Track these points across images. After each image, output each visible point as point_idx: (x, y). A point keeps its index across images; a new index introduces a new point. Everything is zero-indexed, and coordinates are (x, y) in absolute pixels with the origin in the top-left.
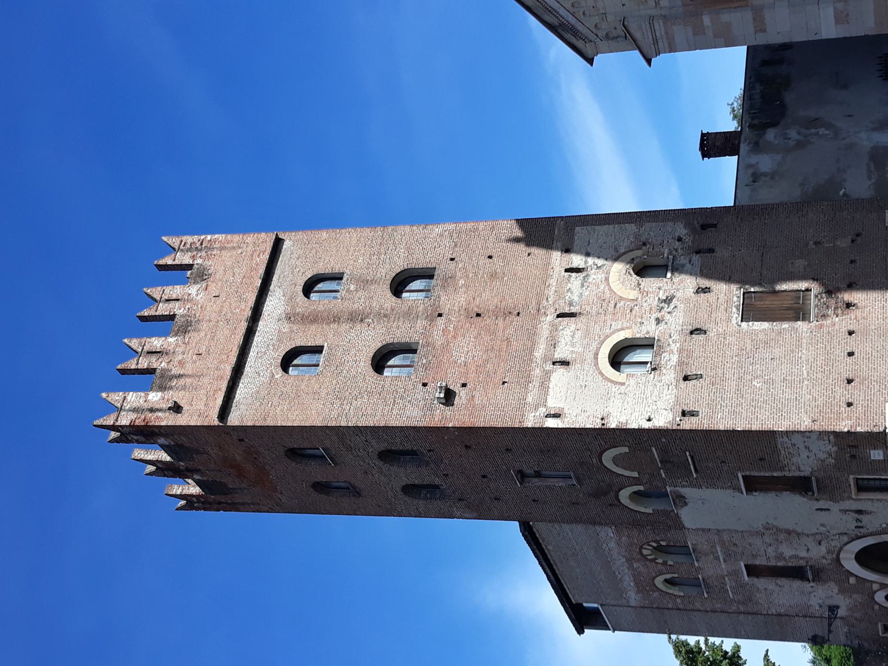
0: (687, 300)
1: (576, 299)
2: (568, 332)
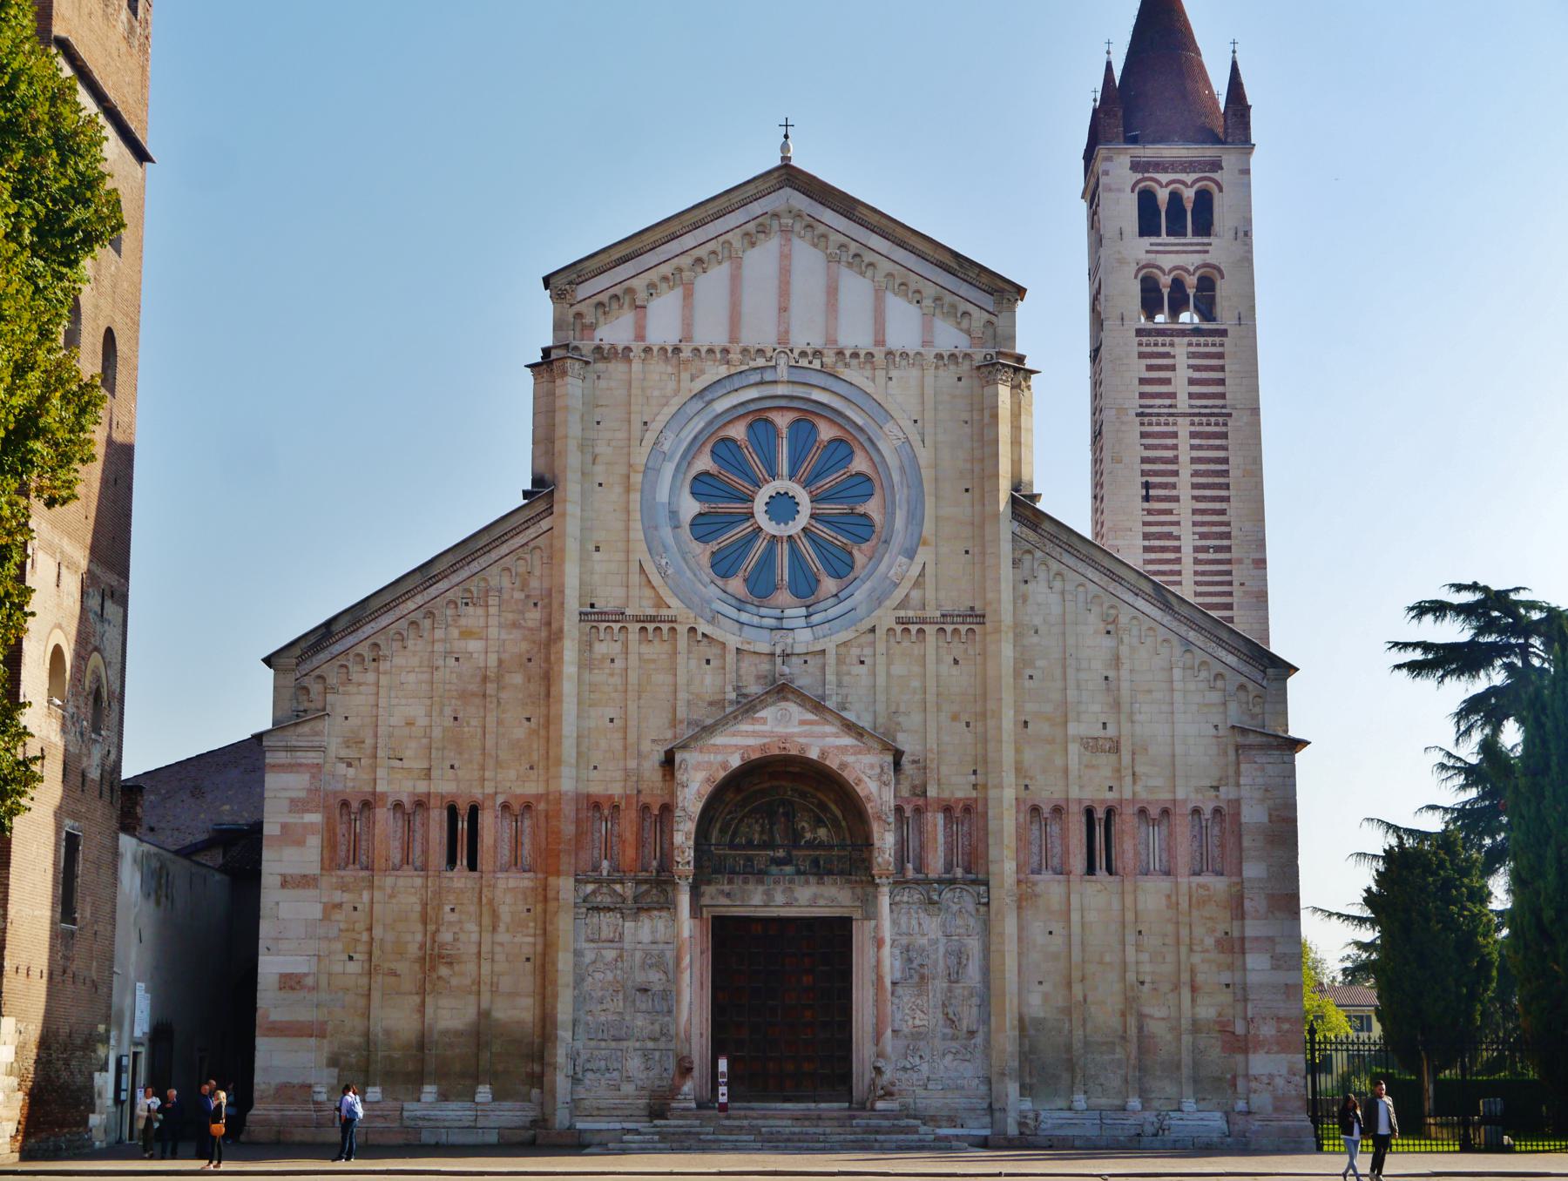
0: (80, 761)
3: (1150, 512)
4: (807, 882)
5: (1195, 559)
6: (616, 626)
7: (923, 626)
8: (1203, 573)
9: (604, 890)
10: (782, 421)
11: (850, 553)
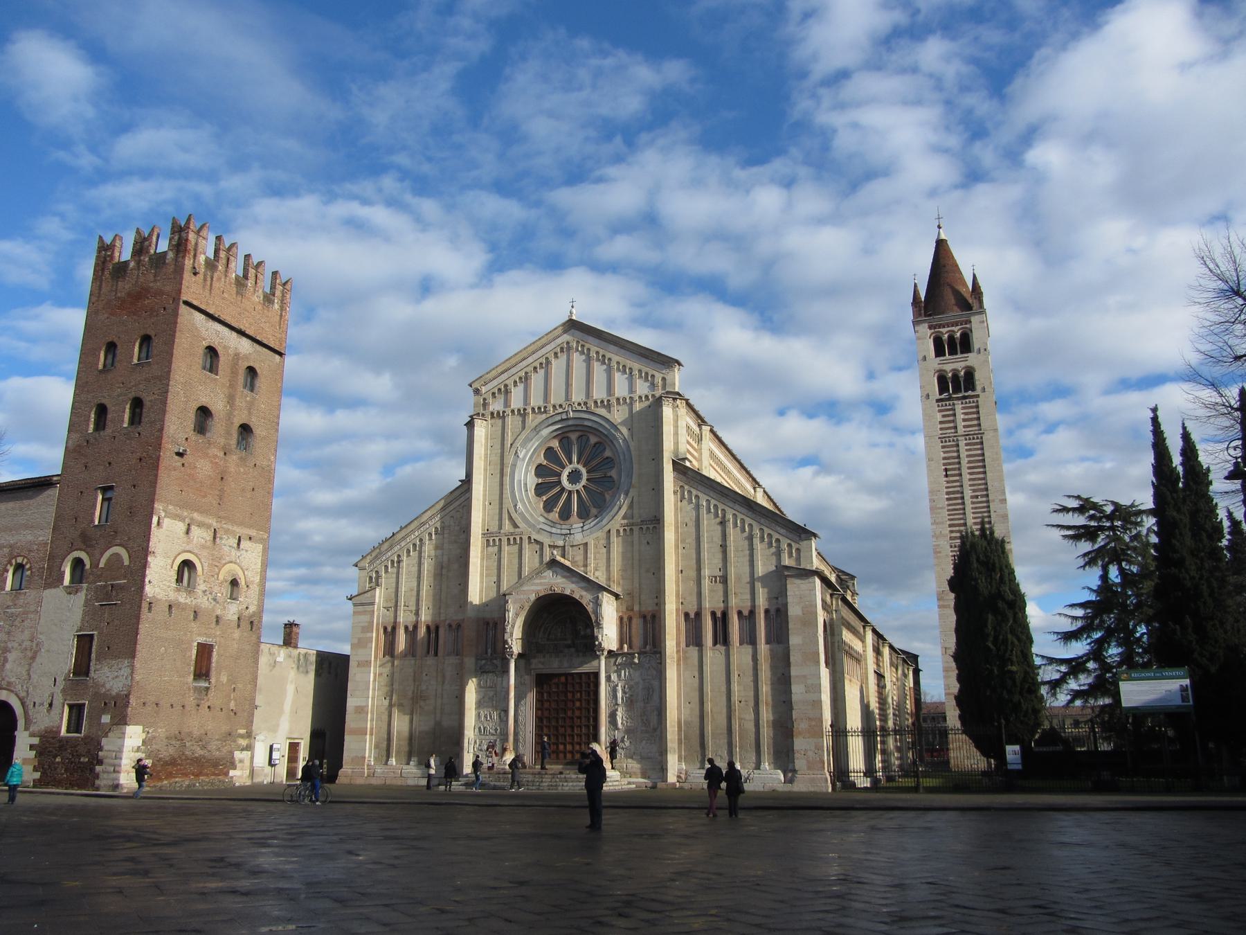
1: (223, 542)
2: (205, 535)
3: (948, 482)
4: (578, 656)
5: (972, 502)
7: (633, 527)
8: (976, 508)
9: (489, 663)
10: (574, 436)
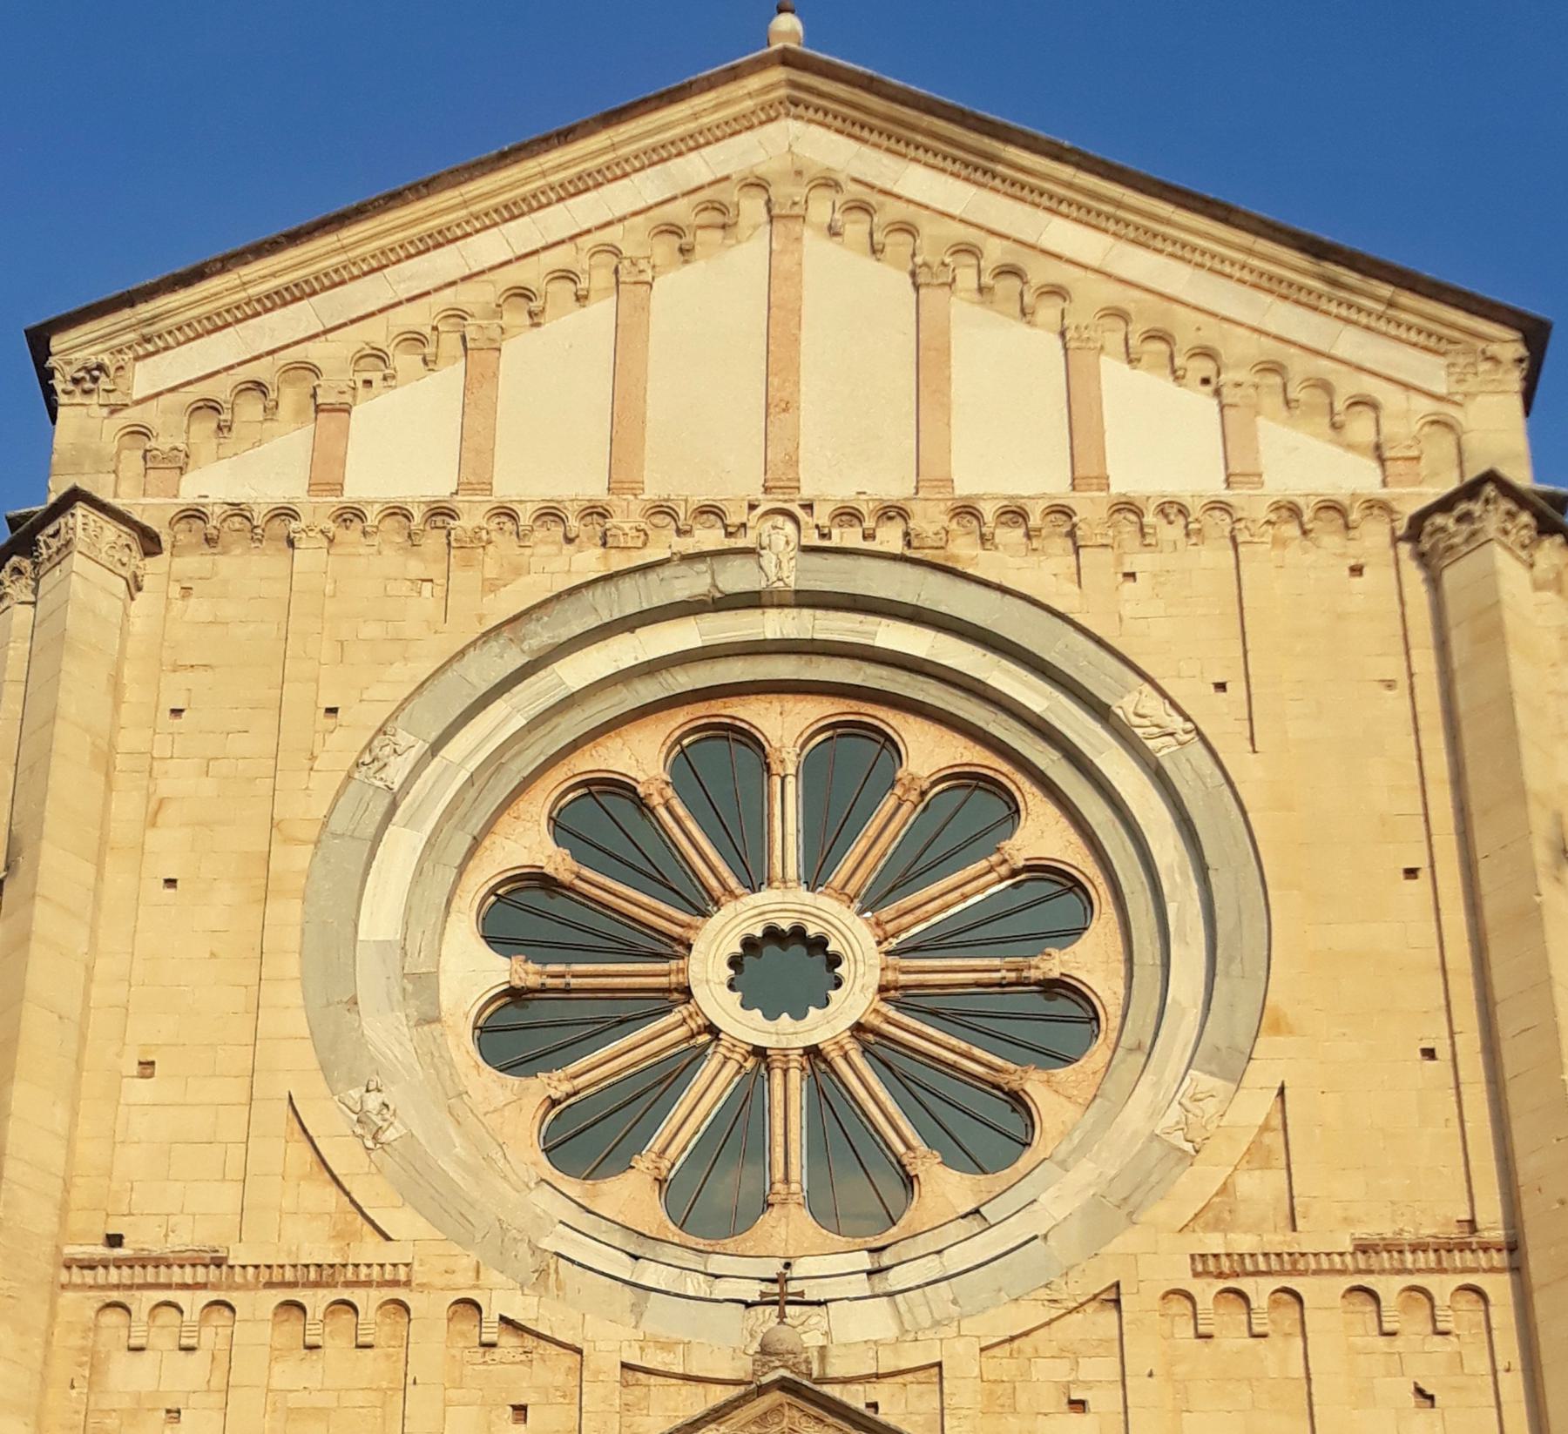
6: (193, 1302)
11: (1017, 1101)
